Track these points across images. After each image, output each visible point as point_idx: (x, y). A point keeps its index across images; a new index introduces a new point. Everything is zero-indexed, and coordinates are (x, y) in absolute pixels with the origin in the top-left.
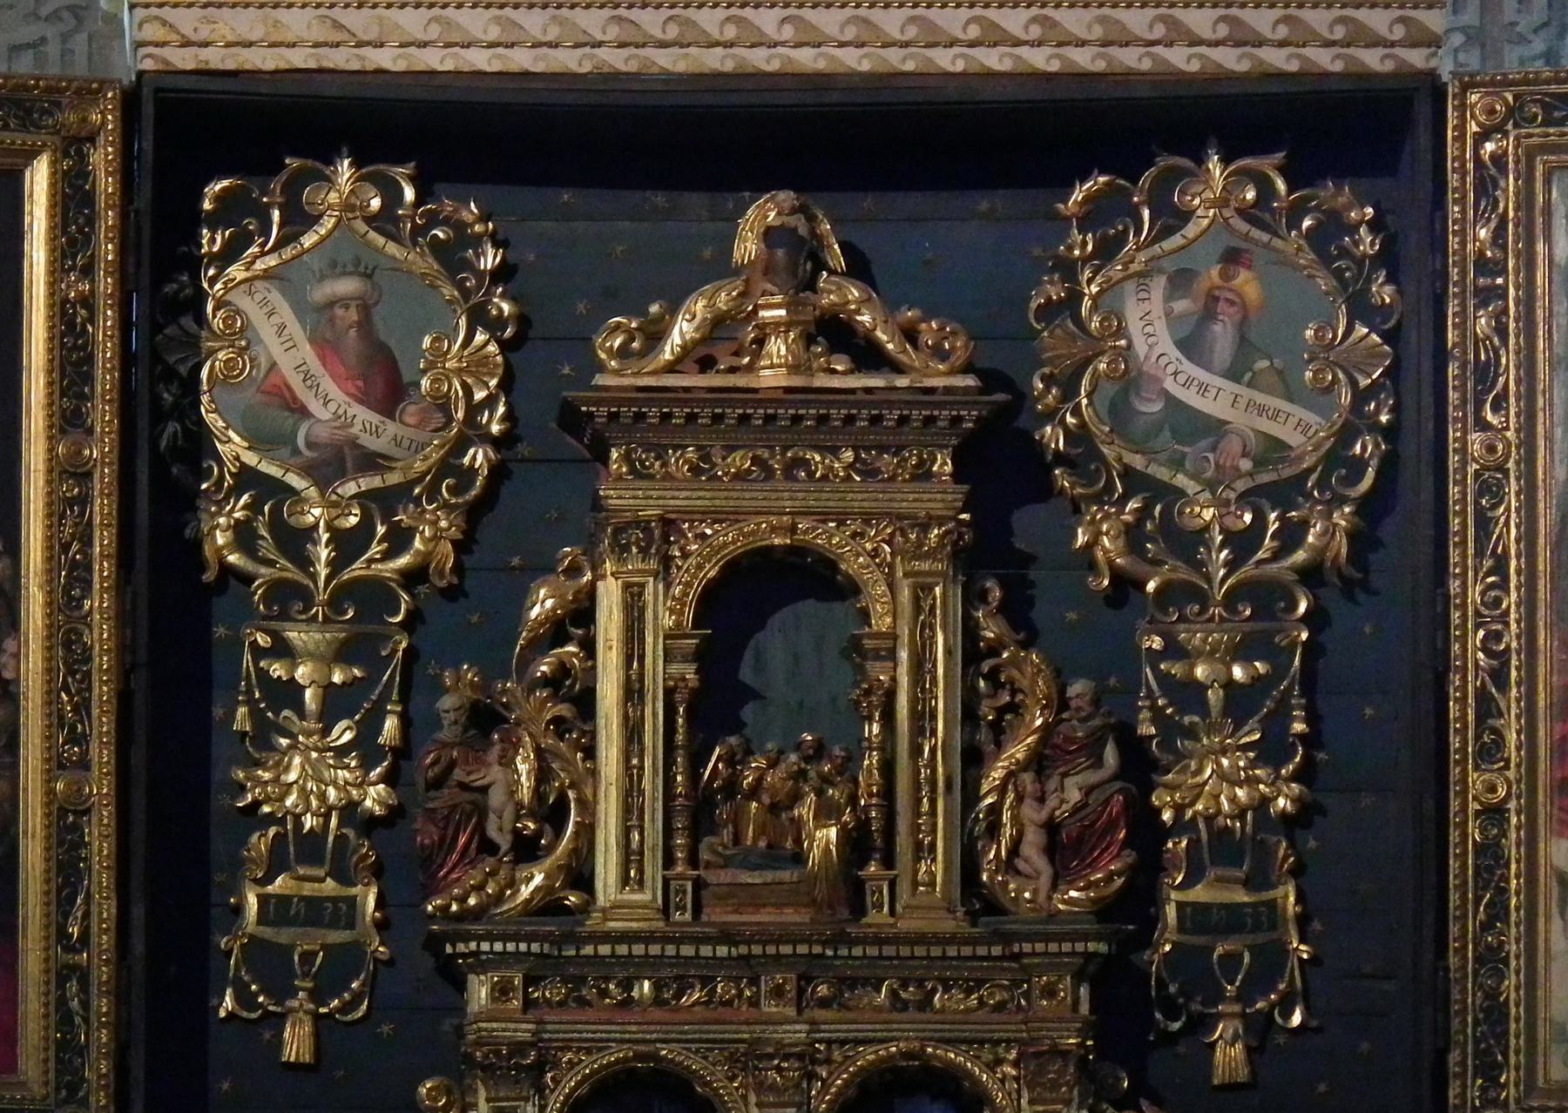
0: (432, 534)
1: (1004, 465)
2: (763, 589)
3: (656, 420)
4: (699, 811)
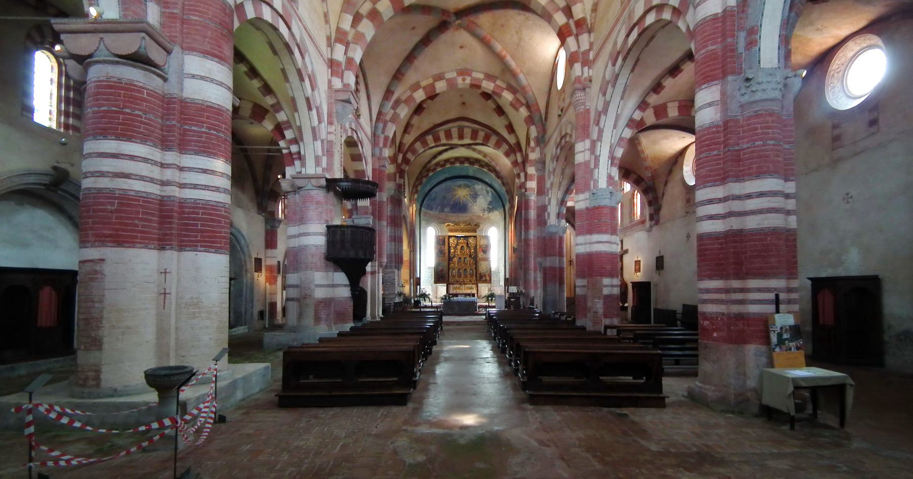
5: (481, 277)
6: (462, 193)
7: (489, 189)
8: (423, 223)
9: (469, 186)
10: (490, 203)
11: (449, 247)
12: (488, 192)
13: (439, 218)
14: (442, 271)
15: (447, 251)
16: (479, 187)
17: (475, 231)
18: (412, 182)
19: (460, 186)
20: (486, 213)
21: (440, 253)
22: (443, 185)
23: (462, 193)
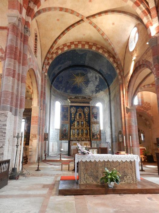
5: (93, 136)
6: (79, 80)
7: (98, 75)
8: (52, 96)
9: (83, 75)
12: (96, 78)
13: (63, 96)
14: (65, 131)
16: (91, 75)
17: (89, 103)
18: (45, 54)
19: (78, 75)
20: (94, 94)
22: (67, 72)
23: (79, 80)
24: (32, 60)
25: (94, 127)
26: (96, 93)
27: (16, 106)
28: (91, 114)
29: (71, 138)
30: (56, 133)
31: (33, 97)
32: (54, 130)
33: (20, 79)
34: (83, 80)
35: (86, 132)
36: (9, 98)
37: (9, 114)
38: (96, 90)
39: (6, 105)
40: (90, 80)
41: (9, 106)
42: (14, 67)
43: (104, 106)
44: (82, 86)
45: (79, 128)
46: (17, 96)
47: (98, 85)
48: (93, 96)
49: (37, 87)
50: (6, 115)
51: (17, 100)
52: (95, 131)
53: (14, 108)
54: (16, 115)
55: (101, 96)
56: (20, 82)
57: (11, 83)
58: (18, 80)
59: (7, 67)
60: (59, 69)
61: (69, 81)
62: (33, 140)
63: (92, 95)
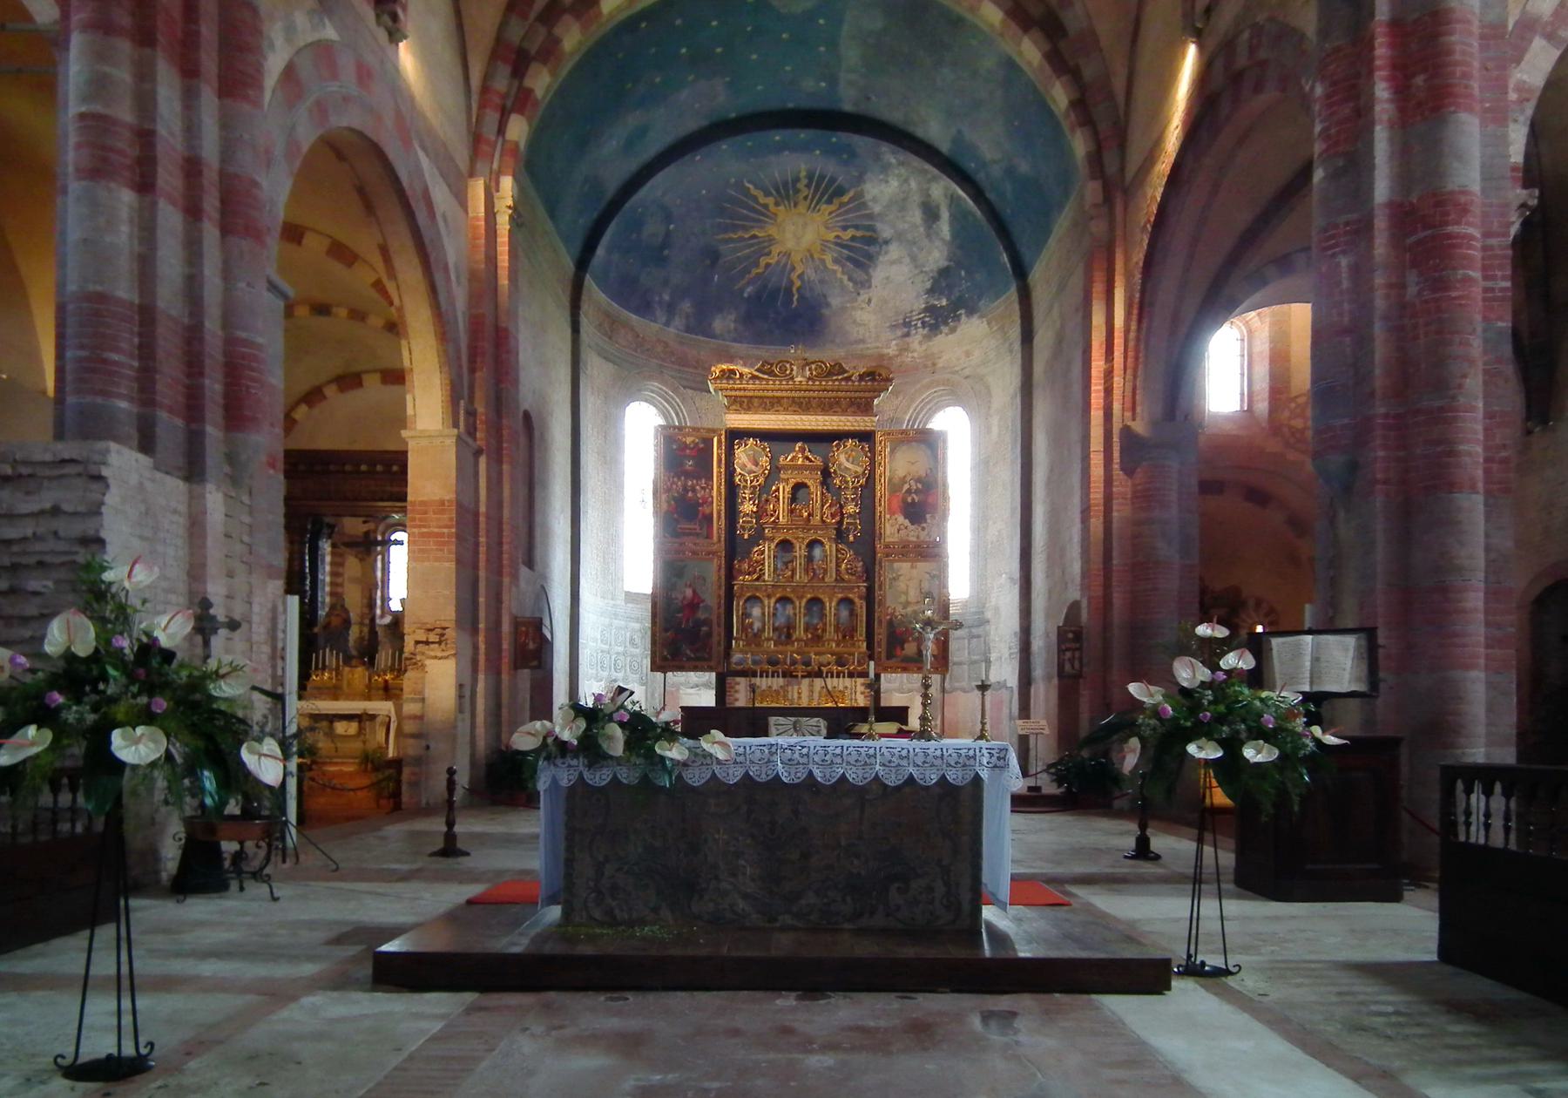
0: (761, 480)
1: (826, 474)
2: (799, 487)
3: (786, 468)
4: (792, 511)
9: (827, 191)
10: (942, 281)
11: (732, 490)
12: (931, 214)
14: (693, 605)
15: (717, 506)
17: (865, 408)
19: (786, 192)
20: (916, 340)
21: (680, 512)
23: (799, 237)
24: (346, 63)
25: (902, 585)
26: (934, 329)
27: (193, 409)
28: (880, 489)
29: (736, 657)
30: (637, 626)
31: (406, 363)
32: (621, 601)
33: (211, 203)
34: (831, 236)
35: (844, 613)
36: (117, 350)
37: (124, 463)
38: (930, 309)
39: (99, 400)
40: (885, 232)
41: (123, 404)
42: (145, 103)
43: (989, 430)
44: (822, 282)
45: (794, 590)
46: (193, 335)
47: (944, 273)
48: (907, 358)
49: (433, 289)
50: (93, 470)
51: (194, 366)
52: (909, 610)
53: (170, 425)
54: (193, 470)
55: (968, 354)
56: (210, 232)
57: (123, 236)
58: (193, 212)
59: (83, 109)
60: (629, 145)
61: (723, 248)
62: (428, 662)
63: (904, 349)
